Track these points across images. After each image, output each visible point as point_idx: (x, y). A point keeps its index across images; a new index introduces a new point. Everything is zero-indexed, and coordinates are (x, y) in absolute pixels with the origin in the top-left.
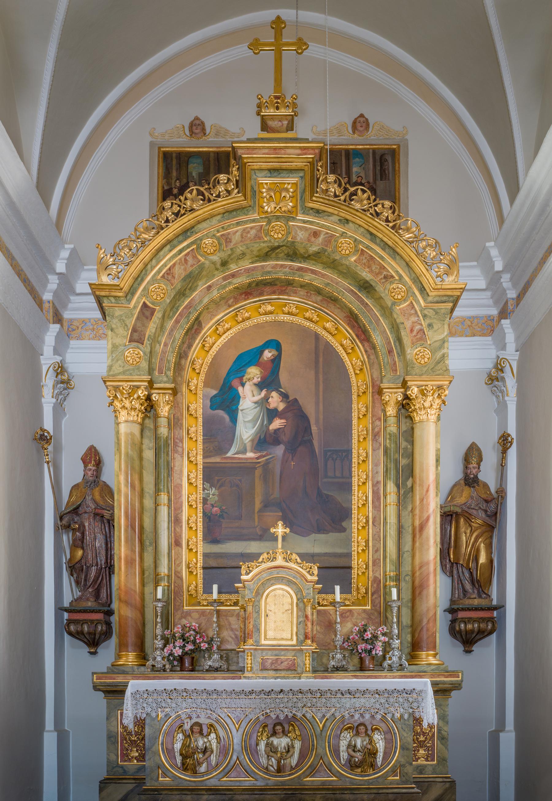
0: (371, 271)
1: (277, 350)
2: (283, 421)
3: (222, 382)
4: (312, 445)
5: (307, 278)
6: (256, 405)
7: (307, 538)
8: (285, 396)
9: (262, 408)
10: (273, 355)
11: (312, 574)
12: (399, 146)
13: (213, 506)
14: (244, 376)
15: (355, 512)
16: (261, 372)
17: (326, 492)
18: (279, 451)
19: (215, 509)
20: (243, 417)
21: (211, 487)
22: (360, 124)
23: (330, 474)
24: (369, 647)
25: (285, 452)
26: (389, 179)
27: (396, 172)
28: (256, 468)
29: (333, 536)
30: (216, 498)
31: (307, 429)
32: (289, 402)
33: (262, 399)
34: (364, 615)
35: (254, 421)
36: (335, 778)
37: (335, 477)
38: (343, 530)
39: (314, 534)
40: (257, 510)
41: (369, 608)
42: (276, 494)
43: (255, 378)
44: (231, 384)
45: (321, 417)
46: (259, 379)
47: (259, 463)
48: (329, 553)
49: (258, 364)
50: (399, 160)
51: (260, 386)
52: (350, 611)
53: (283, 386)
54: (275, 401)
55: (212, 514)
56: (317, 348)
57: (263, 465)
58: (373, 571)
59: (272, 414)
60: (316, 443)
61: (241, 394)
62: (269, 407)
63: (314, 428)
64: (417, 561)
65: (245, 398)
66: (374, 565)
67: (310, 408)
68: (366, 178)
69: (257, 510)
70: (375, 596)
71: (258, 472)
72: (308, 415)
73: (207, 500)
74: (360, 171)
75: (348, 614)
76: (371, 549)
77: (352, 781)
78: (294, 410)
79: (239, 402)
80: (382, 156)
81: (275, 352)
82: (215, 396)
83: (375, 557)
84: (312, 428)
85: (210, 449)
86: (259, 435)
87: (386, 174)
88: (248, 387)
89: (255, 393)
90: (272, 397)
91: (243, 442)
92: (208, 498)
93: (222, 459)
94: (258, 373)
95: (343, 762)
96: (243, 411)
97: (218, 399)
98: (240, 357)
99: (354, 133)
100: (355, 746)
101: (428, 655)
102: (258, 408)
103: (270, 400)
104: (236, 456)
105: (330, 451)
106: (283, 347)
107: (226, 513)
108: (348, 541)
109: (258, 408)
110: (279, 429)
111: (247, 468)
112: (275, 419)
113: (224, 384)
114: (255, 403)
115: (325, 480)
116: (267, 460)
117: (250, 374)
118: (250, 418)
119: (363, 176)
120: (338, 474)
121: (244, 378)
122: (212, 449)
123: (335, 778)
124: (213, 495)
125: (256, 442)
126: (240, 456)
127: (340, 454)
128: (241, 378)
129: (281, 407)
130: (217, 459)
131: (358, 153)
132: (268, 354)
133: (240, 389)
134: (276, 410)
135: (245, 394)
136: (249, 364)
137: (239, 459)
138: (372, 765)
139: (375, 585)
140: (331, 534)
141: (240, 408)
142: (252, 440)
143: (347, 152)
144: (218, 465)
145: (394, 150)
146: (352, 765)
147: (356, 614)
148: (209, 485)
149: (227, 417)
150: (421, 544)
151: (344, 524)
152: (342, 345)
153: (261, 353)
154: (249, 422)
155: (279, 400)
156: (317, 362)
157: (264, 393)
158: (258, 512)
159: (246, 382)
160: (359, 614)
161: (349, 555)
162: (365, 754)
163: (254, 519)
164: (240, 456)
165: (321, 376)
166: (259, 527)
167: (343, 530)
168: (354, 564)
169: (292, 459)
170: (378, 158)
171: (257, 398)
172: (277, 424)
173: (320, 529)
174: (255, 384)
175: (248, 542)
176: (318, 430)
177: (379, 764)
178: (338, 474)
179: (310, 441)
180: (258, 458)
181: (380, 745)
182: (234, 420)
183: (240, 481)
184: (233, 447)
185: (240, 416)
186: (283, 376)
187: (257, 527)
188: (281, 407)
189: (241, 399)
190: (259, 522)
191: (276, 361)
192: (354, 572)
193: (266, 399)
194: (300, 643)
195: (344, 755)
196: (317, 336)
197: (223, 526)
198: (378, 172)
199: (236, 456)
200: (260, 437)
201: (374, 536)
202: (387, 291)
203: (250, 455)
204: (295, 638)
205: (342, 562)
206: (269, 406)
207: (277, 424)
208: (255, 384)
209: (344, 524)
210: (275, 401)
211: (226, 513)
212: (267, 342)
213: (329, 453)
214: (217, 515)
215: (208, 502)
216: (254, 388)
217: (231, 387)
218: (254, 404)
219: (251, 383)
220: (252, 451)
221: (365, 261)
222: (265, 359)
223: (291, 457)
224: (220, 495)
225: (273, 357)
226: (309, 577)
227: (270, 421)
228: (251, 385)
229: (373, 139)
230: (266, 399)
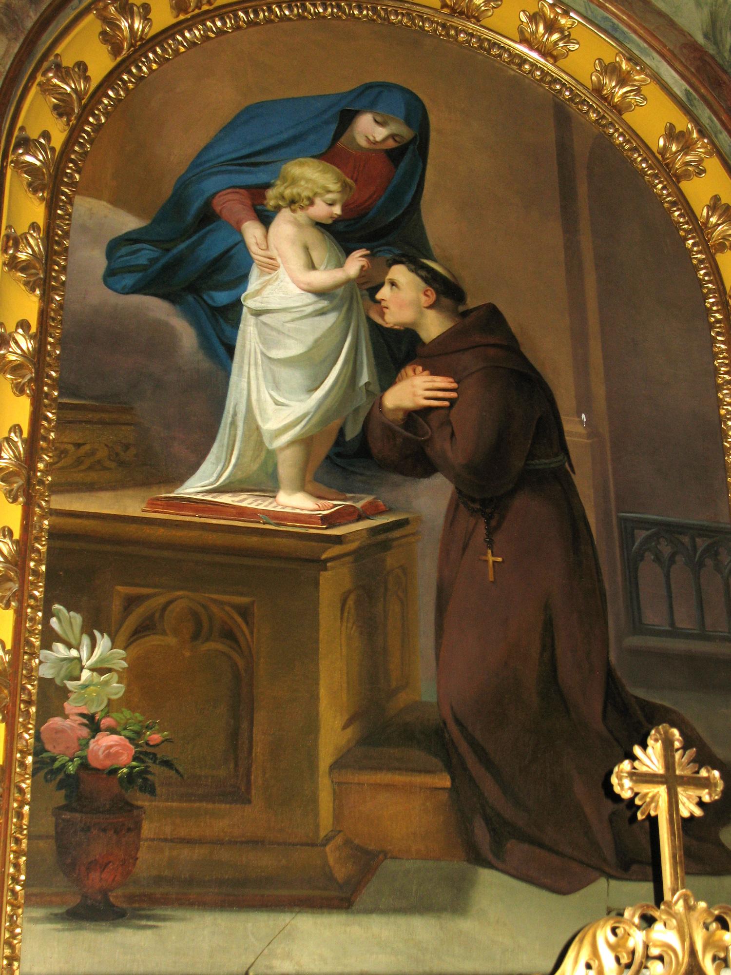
1: (408, 122)
3: (167, 189)
6: (323, 304)
7: (575, 897)
8: (446, 290)
9: (348, 319)
10: (392, 136)
13: (93, 725)
14: (268, 186)
16: (345, 186)
17: (640, 693)
18: (430, 499)
19: (106, 741)
20: (265, 341)
21: (88, 628)
23: (653, 616)
28: (322, 565)
30: (117, 688)
31: (549, 427)
32: (465, 314)
33: (348, 283)
35: (314, 364)
37: (674, 633)
39: (602, 882)
40: (326, 756)
42: (424, 685)
43: (318, 201)
44: (208, 203)
45: (599, 390)
46: (337, 210)
47: (338, 540)
49: (330, 155)
51: (342, 234)
53: (436, 252)
55: (84, 766)
57: (358, 555)
61: (254, 249)
62: (379, 321)
63: (575, 427)
65: (274, 268)
69: (326, 756)
71: (333, 584)
73: (65, 693)
79: (243, 279)
82: (130, 239)
84: (567, 427)
85: (93, 453)
86: (336, 423)
88: (285, 227)
89: (316, 255)
90: (393, 284)
91: (260, 443)
92: (70, 685)
93: (154, 503)
94: (334, 186)
96: (263, 318)
97: (146, 254)
98: (249, 115)
102: (331, 319)
103: (385, 293)
104: (226, 499)
105: (645, 524)
106: (432, 118)
107: (167, 764)
109: (331, 319)
110: (425, 412)
111: (270, 563)
112: (409, 370)
113: (177, 202)
114: (321, 293)
116: (374, 531)
117: (294, 182)
118: (294, 349)
120: (684, 620)
121: (271, 193)
122: (103, 453)
124: (100, 670)
125: (323, 449)
126: (247, 501)
127: (686, 540)
128: (257, 192)
130: (131, 504)
132: (370, 130)
133: (252, 231)
135: (274, 253)
136: (292, 145)
137: (241, 512)
141: (250, 303)
142: (306, 442)
144: (131, 530)
148: (77, 619)
149: (186, 335)
153: (347, 118)
154: (289, 362)
155: (424, 301)
157: (355, 264)
158: (337, 766)
159: (278, 208)
163: (314, 800)
164: (247, 501)
165: (586, 242)
166: (339, 840)
169: (490, 544)
171: (325, 277)
172: (415, 389)
174: (319, 225)
175: (284, 919)
176: (589, 436)
178: (684, 620)
180: (329, 520)
182: (221, 345)
183: (245, 612)
184: (211, 458)
185: (249, 335)
186: (438, 220)
187: (328, 840)
189: (255, 272)
190: (338, 816)
191: (409, 155)
193: (368, 286)
197: (147, 829)
199: (226, 499)
200: (341, 432)
203: (294, 502)
206: (382, 315)
207: (415, 389)
208: (319, 225)
211: (167, 764)
212: (370, 86)
213: (641, 535)
214: (114, 771)
215: (70, 706)
216: (313, 237)
217: (208, 216)
218: (311, 298)
219: (301, 215)
220: (302, 487)
222: (363, 142)
223: (481, 530)
224: (138, 676)
225: (391, 144)
227: (388, 375)
228: (297, 224)
230: (368, 286)
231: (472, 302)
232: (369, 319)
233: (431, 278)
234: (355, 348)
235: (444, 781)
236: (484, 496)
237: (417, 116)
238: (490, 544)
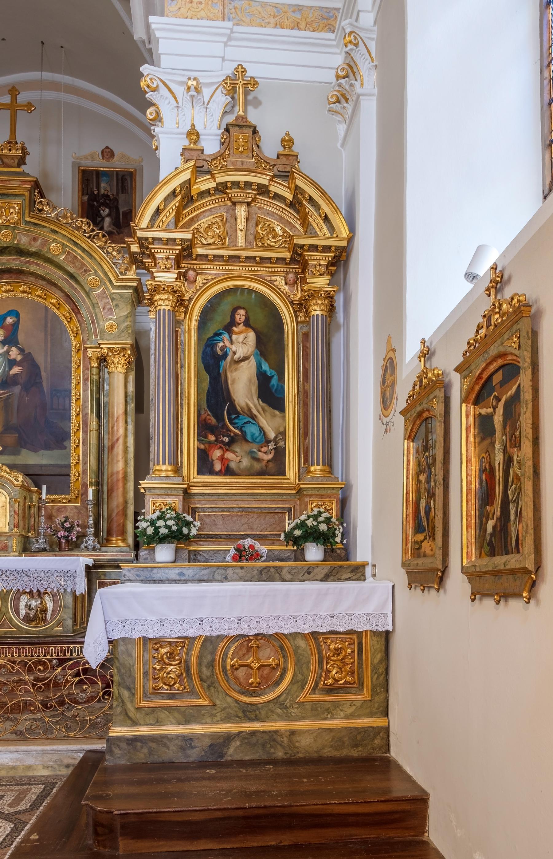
0: (75, 267)
2: (20, 368)
4: (42, 386)
5: (32, 268)
8: (21, 351)
11: (18, 481)
12: (136, 170)
15: (73, 435)
18: (17, 389)
24: (67, 534)
25: (21, 391)
26: (128, 193)
27: (133, 189)
29: (56, 452)
31: (39, 374)
33: (5, 352)
34: (75, 510)
36: (14, 629)
38: (65, 448)
41: (79, 505)
42: (14, 421)
48: (53, 465)
50: (135, 180)
52: (65, 507)
53: (20, 343)
54: (14, 353)
56: (46, 317)
57: (5, 400)
58: (82, 478)
59: (12, 363)
60: (44, 384)
63: (43, 374)
64: (110, 472)
66: (83, 474)
67: (40, 359)
68: (111, 192)
70: (84, 496)
72: (39, 365)
74: (106, 186)
75: (63, 509)
76: (81, 461)
77: (27, 632)
78: (28, 360)
80: (123, 176)
81: (15, 319)
83: (84, 468)
87: (126, 190)
94: (2, 333)
95: (22, 618)
99: (103, 158)
100: (30, 606)
101: (117, 540)
103: (11, 353)
108: (68, 456)
115: (51, 411)
119: (109, 190)
123: (14, 629)
129: (19, 358)
131: (105, 173)
134: (15, 360)
138: (44, 620)
139: (84, 489)
140: (55, 450)
143: (98, 172)
145: (132, 172)
146: (28, 619)
147: (69, 510)
150: (112, 460)
151: (65, 443)
152: (64, 316)
153: (5, 319)
155: (18, 353)
156: (46, 326)
157: (6, 348)
160: (71, 509)
161: (68, 466)
162: (37, 611)
165: (49, 337)
167: (65, 448)
168: (73, 472)
170: (120, 177)
172: (16, 370)
173: (47, 447)
177: (48, 618)
179: (41, 383)
181: (50, 606)
186: (21, 337)
188: (19, 358)
191: (16, 325)
192: (72, 479)
193: (8, 352)
194: (11, 530)
195: (23, 612)
196: (46, 308)
198: (120, 188)
201: (83, 452)
202: (86, 281)
204: (7, 527)
205: (64, 471)
207: (16, 370)
209: (65, 443)
210: (14, 353)
212: (10, 311)
221: (70, 259)
226: (16, 483)
227: (10, 369)
229: (117, 164)
230: (8, 352)
231: (26, 352)
232: (8, 359)
233: (19, 349)
234: (5, 364)
235: (17, 435)
236: (26, 388)
237: (17, 315)
238: (27, 396)
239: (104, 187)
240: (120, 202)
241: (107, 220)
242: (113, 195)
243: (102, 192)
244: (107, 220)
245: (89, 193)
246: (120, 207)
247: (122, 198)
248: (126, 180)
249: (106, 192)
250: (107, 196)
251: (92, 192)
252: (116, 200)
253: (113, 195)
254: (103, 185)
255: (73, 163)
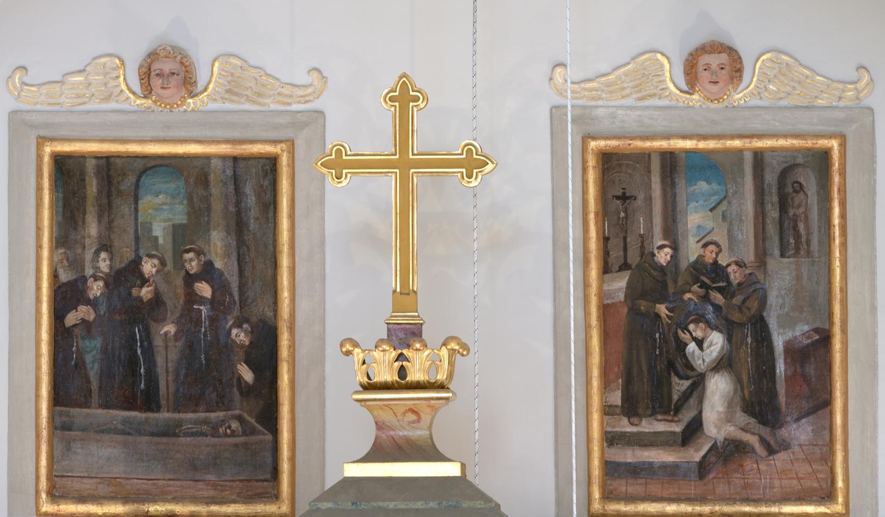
22: (713, 62)
26: (809, 253)
68: (731, 248)
74: (710, 224)
87: (797, 237)
131: (707, 165)
143: (670, 159)
170: (771, 178)
198: (772, 230)
239: (704, 228)
240: (773, 299)
241: (719, 387)
242: (740, 264)
243: (692, 251)
244: (719, 387)
245: (634, 258)
246: (773, 323)
247: (780, 280)
248: (799, 188)
249: (709, 256)
250: (717, 271)
251: (647, 256)
252: (755, 288)
253: (740, 264)
254: (695, 219)
255: (17, 122)
